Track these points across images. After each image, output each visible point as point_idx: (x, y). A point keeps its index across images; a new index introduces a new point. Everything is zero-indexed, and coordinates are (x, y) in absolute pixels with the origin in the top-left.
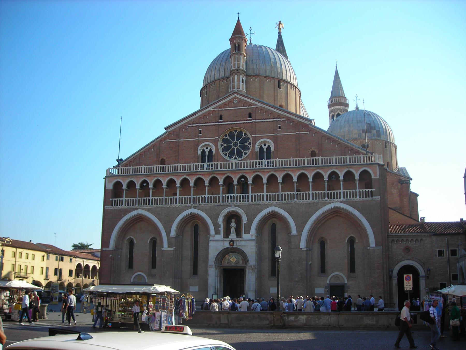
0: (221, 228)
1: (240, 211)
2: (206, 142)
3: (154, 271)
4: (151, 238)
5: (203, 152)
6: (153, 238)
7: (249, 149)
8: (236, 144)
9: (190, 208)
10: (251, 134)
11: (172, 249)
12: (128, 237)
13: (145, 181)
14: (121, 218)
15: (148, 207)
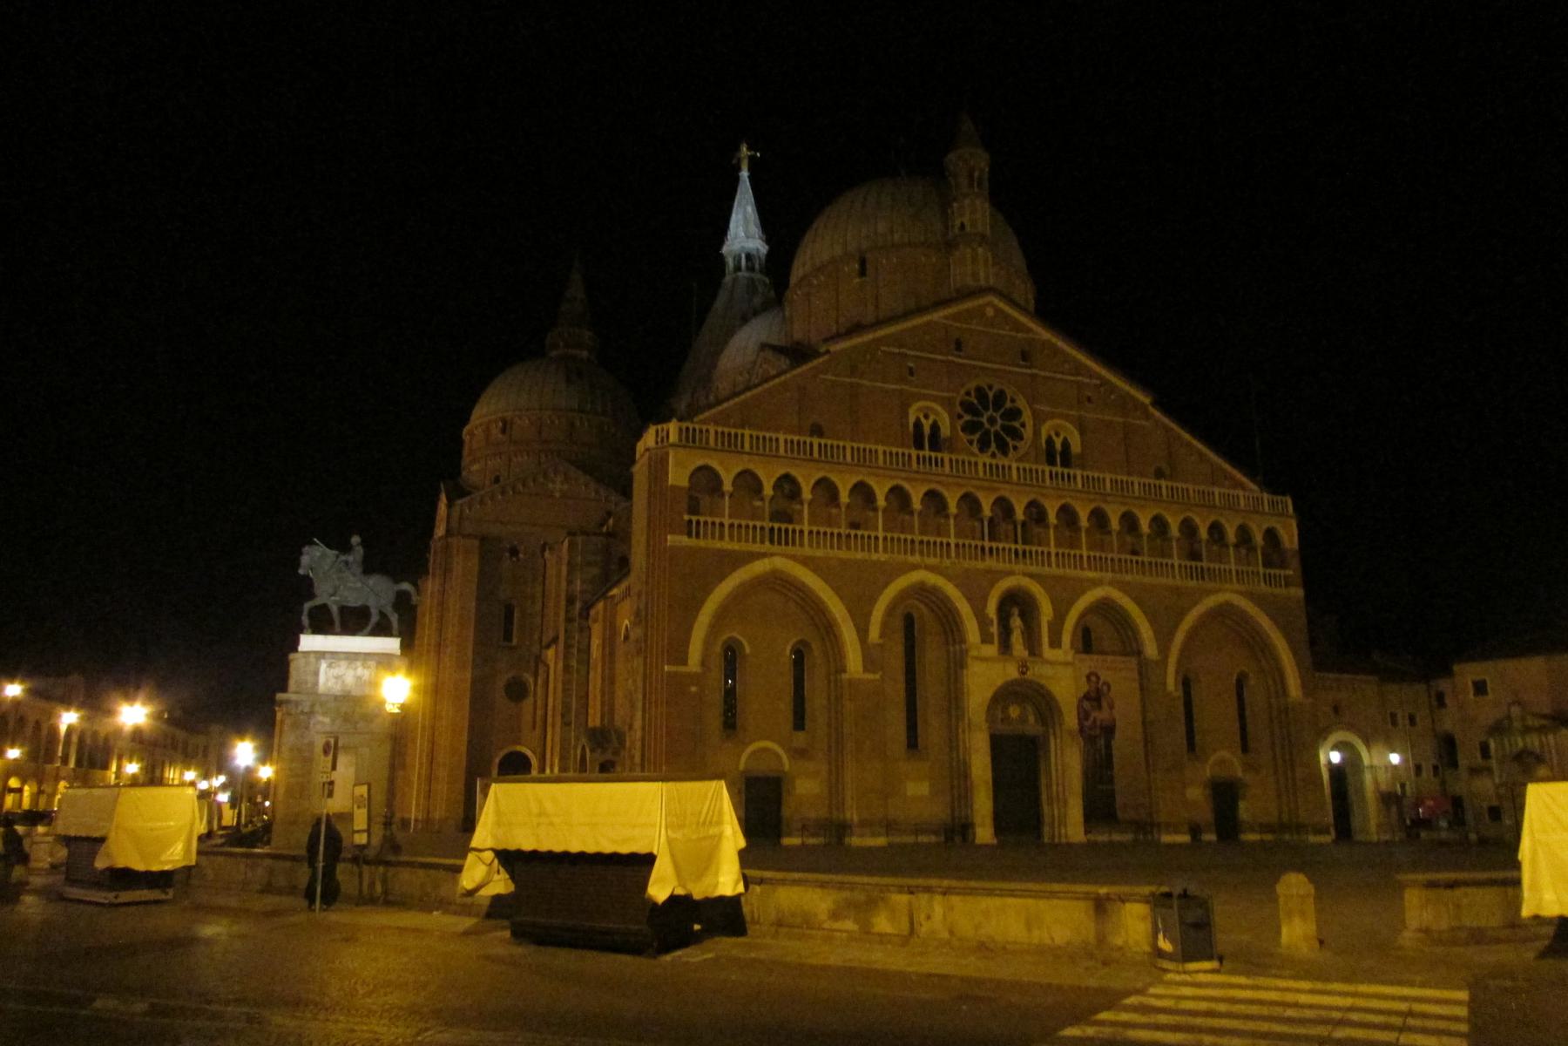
0: (994, 629)
1: (1036, 590)
2: (926, 400)
3: (800, 739)
4: (795, 640)
5: (918, 425)
6: (802, 642)
7: (1021, 438)
8: (992, 421)
9: (915, 567)
10: (1032, 400)
11: (877, 676)
12: (724, 637)
13: (787, 478)
14: (722, 577)
15: (795, 550)
